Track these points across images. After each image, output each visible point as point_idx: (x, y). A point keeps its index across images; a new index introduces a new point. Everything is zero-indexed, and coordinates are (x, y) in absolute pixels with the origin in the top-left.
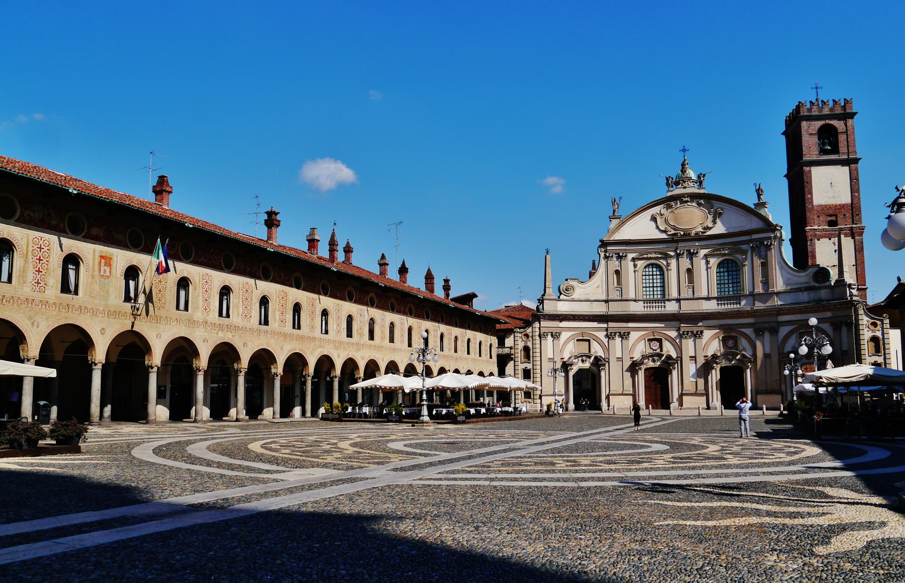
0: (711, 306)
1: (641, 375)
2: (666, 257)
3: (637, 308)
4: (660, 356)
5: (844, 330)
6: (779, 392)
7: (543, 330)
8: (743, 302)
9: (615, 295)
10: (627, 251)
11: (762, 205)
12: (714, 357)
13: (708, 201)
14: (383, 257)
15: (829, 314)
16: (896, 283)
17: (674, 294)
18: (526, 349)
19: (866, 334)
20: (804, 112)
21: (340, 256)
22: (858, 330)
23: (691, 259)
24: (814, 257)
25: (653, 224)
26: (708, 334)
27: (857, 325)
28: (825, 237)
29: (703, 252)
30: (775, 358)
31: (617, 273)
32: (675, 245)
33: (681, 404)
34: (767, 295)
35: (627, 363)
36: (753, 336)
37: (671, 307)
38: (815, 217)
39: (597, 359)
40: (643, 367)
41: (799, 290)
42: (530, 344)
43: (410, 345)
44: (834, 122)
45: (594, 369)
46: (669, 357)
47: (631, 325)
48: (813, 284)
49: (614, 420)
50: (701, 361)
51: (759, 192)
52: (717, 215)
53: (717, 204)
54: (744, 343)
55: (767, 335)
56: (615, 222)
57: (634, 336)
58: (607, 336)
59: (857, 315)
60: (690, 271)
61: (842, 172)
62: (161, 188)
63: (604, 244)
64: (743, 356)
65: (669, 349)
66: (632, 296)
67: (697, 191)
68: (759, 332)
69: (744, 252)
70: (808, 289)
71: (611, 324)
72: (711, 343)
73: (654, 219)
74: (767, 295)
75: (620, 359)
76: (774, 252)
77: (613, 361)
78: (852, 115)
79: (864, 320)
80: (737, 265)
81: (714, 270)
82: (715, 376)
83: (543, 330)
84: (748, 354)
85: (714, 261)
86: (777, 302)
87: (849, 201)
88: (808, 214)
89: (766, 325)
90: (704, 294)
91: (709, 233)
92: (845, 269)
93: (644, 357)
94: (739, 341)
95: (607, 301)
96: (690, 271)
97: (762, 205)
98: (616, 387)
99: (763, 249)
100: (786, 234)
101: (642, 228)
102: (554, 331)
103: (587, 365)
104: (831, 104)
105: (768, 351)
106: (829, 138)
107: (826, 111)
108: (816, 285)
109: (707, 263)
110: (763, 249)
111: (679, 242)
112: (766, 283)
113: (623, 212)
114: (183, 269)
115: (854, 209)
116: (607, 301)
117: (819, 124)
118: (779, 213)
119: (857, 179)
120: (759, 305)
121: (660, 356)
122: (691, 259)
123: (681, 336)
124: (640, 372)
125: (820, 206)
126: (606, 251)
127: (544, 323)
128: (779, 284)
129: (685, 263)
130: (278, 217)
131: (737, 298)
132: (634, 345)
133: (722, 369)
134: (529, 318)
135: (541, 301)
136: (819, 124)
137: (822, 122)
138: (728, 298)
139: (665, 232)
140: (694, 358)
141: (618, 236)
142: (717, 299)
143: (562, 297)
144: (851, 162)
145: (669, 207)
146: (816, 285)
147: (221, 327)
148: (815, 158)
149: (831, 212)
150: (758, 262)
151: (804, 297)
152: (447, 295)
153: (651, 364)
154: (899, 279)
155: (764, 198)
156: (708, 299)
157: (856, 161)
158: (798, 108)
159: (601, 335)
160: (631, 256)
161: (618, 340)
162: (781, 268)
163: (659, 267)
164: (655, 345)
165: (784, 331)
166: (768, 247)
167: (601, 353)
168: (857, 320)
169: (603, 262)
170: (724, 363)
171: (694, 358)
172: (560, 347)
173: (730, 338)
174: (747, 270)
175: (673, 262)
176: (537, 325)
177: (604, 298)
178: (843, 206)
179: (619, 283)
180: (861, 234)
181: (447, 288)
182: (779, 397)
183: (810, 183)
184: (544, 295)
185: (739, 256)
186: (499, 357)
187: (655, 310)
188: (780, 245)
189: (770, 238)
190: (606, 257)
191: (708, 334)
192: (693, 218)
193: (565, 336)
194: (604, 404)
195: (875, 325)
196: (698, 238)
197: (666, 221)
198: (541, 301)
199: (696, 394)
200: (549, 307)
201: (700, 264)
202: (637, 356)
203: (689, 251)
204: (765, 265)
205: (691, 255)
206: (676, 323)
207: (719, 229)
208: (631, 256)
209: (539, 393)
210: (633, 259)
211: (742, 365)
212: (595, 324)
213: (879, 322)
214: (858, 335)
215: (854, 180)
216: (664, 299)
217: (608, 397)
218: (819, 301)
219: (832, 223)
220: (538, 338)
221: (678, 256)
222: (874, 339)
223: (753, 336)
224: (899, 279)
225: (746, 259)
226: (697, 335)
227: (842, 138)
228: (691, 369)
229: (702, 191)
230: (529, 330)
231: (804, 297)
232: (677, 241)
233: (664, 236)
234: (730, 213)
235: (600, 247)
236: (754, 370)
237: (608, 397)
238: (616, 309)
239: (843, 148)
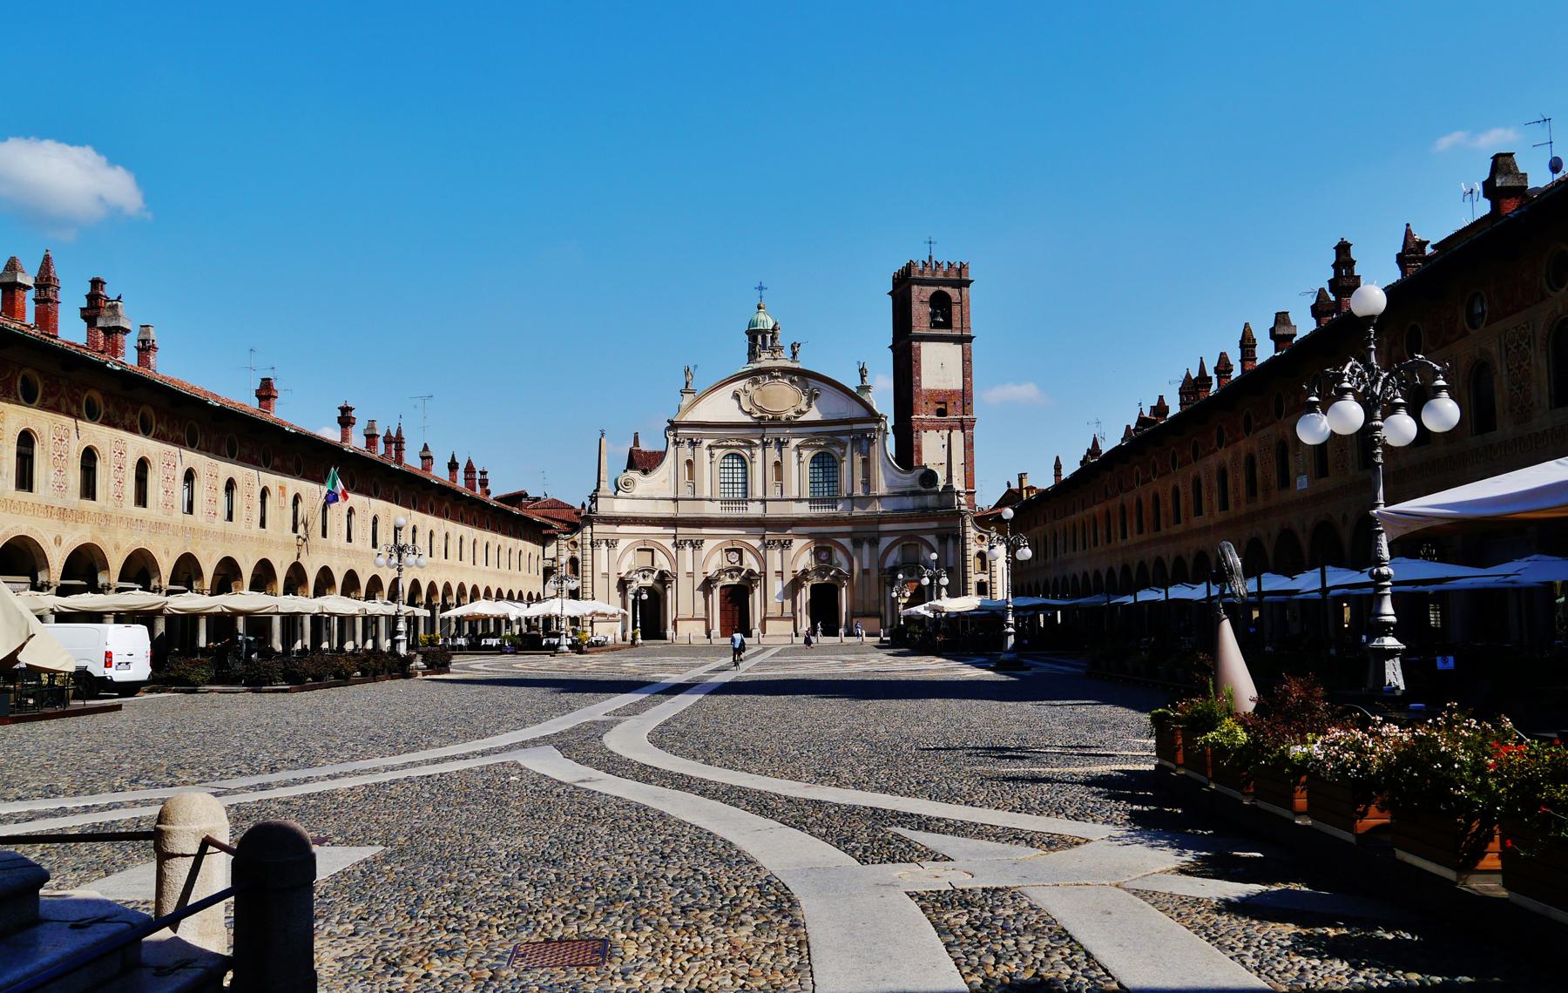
0: (803, 510)
1: (717, 592)
2: (750, 445)
3: (713, 510)
4: (740, 570)
5: (950, 543)
6: (878, 615)
7: (595, 537)
8: (840, 507)
9: (685, 492)
10: (703, 437)
11: (866, 389)
12: (805, 572)
13: (802, 377)
14: (426, 448)
15: (935, 525)
17: (759, 494)
18: (574, 562)
19: (973, 549)
20: (915, 275)
21: (381, 448)
22: (964, 544)
23: (780, 450)
24: (920, 452)
25: (735, 402)
26: (798, 544)
27: (964, 539)
28: (932, 428)
29: (795, 442)
30: (875, 575)
31: (689, 463)
32: (760, 431)
33: (764, 630)
34: (868, 499)
35: (700, 580)
36: (850, 548)
37: (755, 510)
39: (662, 573)
40: (719, 584)
41: (903, 494)
42: (578, 555)
43: (375, 545)
44: (948, 290)
45: (659, 587)
46: (751, 572)
47: (705, 531)
48: (919, 488)
49: (690, 649)
50: (789, 577)
51: (863, 373)
52: (812, 397)
53: (813, 383)
54: (839, 556)
55: (866, 547)
56: (688, 398)
57: (709, 545)
58: (675, 545)
59: (964, 527)
60: (778, 465)
61: (956, 349)
62: (266, 393)
63: (673, 426)
64: (839, 572)
65: (750, 562)
66: (707, 494)
67: (790, 365)
69: (843, 445)
70: (914, 493)
71: (681, 530)
72: (801, 555)
73: (736, 396)
74: (868, 499)
75: (691, 575)
76: (877, 448)
77: (682, 577)
78: (967, 283)
79: (972, 533)
80: (834, 461)
81: (807, 465)
82: (805, 595)
83: (595, 537)
84: (844, 569)
85: (807, 454)
86: (879, 508)
87: (960, 387)
90: (795, 494)
92: (954, 473)
93: (721, 571)
95: (675, 500)
96: (778, 465)
97: (866, 389)
98: (685, 611)
99: (864, 443)
100: (890, 423)
101: (721, 407)
102: (610, 537)
103: (649, 582)
104: (946, 267)
105: (866, 567)
106: (941, 304)
107: (940, 276)
109: (800, 455)
110: (864, 443)
111: (766, 427)
112: (867, 484)
113: (699, 385)
114: (356, 500)
115: (965, 396)
116: (675, 500)
117: (932, 290)
118: (882, 399)
120: (857, 512)
121: (740, 570)
122: (780, 450)
123: (766, 546)
127: (597, 528)
128: (881, 488)
129: (773, 454)
130: (353, 414)
131: (832, 501)
132: (709, 556)
134: (578, 521)
136: (932, 290)
137: (935, 289)
138: (823, 501)
139: (750, 413)
140: (780, 574)
141: (691, 417)
142: (810, 501)
144: (964, 340)
145: (756, 382)
147: (131, 522)
148: (925, 331)
149: (941, 399)
150: (858, 459)
151: (909, 502)
152: (488, 493)
153: (728, 581)
156: (799, 500)
157: (970, 339)
158: (909, 267)
159: (668, 543)
160: (706, 442)
161: (689, 549)
162: (884, 466)
163: (740, 457)
164: (734, 557)
165: (885, 542)
166: (871, 441)
167: (666, 567)
168: (964, 533)
169: (672, 449)
170: (816, 580)
171: (780, 574)
172: (616, 559)
173: (823, 549)
174: (845, 466)
175: (759, 452)
176: (588, 529)
178: (953, 393)
179: (691, 476)
180: (972, 427)
181: (484, 483)
182: (877, 621)
183: (919, 362)
184: (597, 490)
185: (837, 450)
188: (884, 439)
189: (873, 430)
190: (676, 443)
191: (798, 544)
192: (784, 398)
193: (623, 544)
194: (670, 632)
195: (982, 538)
196: (790, 424)
197: (751, 400)
198: (594, 499)
199: (781, 618)
200: (605, 507)
201: (790, 456)
202: (711, 570)
203: (778, 440)
204: (866, 462)
205: (781, 445)
206: (760, 530)
207: (814, 415)
208: (706, 442)
210: (710, 447)
212: (660, 530)
214: (964, 550)
215: (967, 361)
216: (746, 499)
217: (675, 623)
218: (925, 509)
219: (942, 413)
221: (765, 445)
222: (981, 555)
223: (850, 548)
225: (844, 454)
226: (786, 545)
227: (956, 309)
228: (776, 587)
229: (796, 365)
230: (578, 537)
231: (909, 502)
232: (764, 427)
233: (748, 419)
234: (830, 399)
235: (668, 429)
236: (852, 590)
237: (675, 623)
238: (686, 510)
239: (956, 323)
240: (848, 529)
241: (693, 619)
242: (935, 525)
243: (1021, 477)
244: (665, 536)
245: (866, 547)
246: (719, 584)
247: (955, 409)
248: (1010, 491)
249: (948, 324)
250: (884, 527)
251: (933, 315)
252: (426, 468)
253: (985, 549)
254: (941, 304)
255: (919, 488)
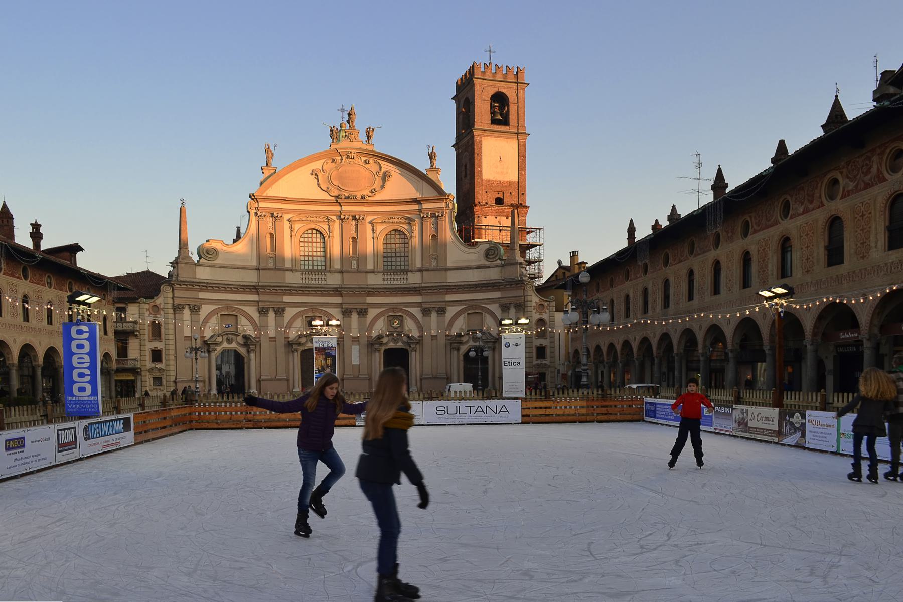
7: (177, 302)
12: (380, 337)
16: (558, 266)
30: (442, 341)
36: (419, 316)
38: (484, 192)
39: (246, 337)
48: (484, 262)
51: (432, 156)
53: (386, 166)
55: (434, 315)
67: (365, 147)
68: (426, 312)
70: (478, 267)
75: (273, 339)
77: (265, 344)
79: (534, 299)
88: (476, 189)
89: (433, 305)
91: (378, 197)
93: (300, 336)
94: (405, 321)
95: (258, 269)
102: (192, 302)
108: (487, 263)
115: (520, 186)
118: (449, 185)
119: (524, 156)
124: (296, 354)
125: (489, 181)
126: (257, 209)
133: (387, 352)
135: (175, 264)
138: (396, 272)
143: (202, 260)
146: (487, 263)
154: (560, 262)
155: (437, 163)
156: (373, 272)
159: (252, 311)
165: (451, 311)
167: (250, 331)
177: (254, 264)
178: (510, 183)
186: (117, 333)
187: (315, 281)
193: (206, 309)
209: (173, 379)
211: (408, 348)
213: (546, 304)
220: (171, 311)
224: (560, 262)
238: (269, 278)
240: (418, 299)
241: (276, 379)
242: (497, 295)
243: (574, 255)
244: (248, 303)
245: (434, 315)
246: (301, 348)
247: (512, 201)
248: (561, 268)
249: (505, 122)
250: (449, 298)
251: (493, 113)
252: (37, 245)
253: (545, 316)
254: (500, 99)
255: (484, 262)
